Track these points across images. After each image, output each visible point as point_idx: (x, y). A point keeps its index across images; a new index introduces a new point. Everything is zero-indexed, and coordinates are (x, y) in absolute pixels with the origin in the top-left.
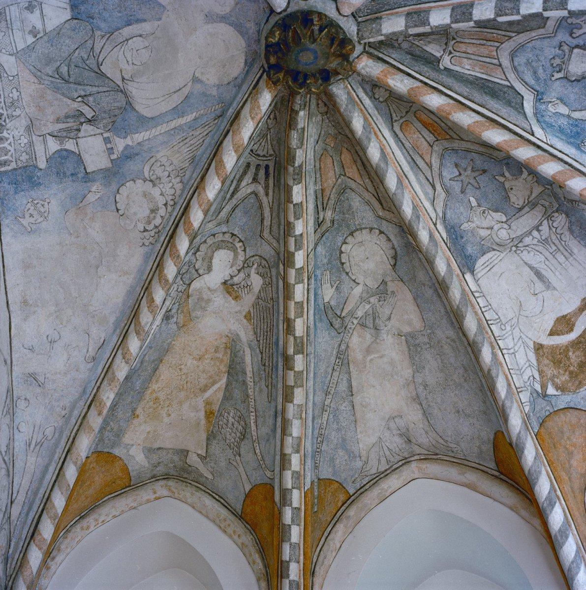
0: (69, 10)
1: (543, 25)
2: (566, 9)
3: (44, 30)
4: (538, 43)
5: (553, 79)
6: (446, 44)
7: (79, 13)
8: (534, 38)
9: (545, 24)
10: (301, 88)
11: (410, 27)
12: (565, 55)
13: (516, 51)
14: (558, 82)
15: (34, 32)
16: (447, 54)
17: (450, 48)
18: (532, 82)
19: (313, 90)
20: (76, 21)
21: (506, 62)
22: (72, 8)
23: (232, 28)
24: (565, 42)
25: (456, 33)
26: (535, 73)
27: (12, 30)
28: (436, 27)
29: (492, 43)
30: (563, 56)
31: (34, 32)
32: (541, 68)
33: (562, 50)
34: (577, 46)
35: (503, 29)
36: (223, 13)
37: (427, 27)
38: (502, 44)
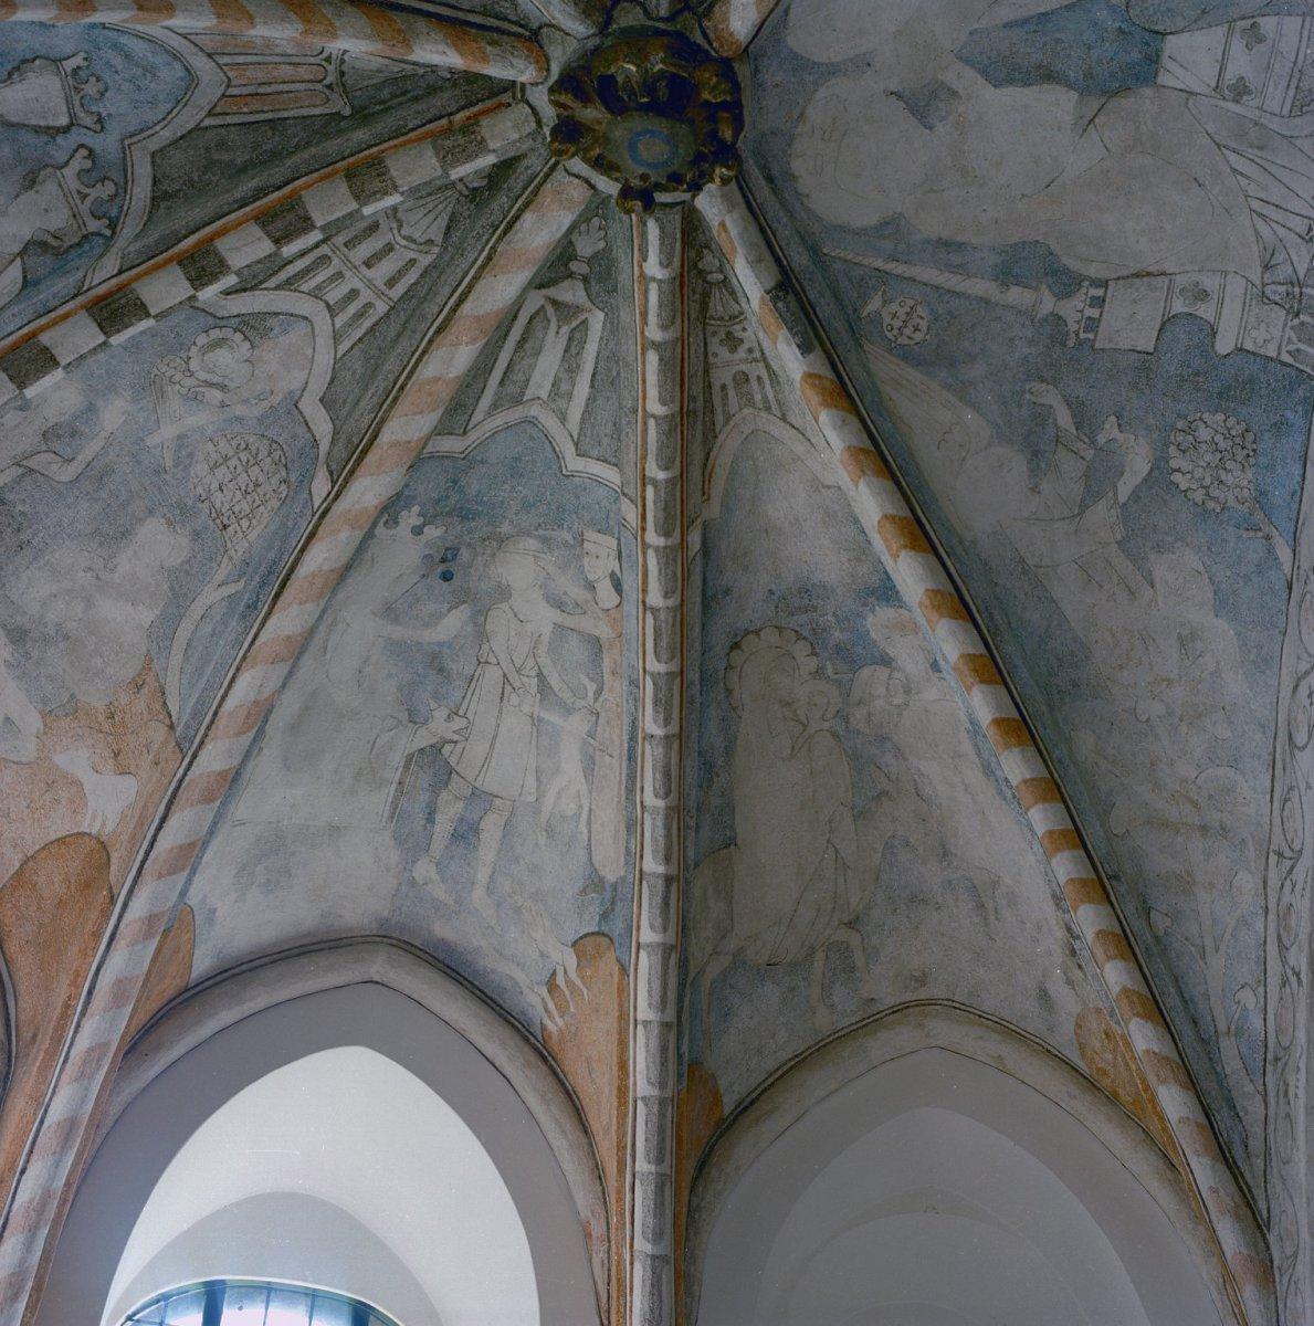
0: (1166, 54)
1: (158, 161)
2: (157, 316)
3: (1230, 32)
4: (150, 116)
5: (82, 55)
6: (342, 74)
7: (1148, 44)
8: (162, 124)
9: (153, 163)
10: (661, 70)
11: (438, 178)
12: (82, 105)
13: (187, 89)
14: (68, 50)
15: (1254, 36)
16: (334, 56)
17: (331, 68)
18: (124, 40)
19: (633, 68)
20: (1159, 28)
21: (201, 63)
22: (1158, 56)
23: (816, 60)
24: (95, 132)
25: (328, 100)
26: (127, 56)
27: (1295, 63)
28: (386, 194)
29: (245, 91)
30: (85, 102)
31: (1254, 36)
32: (120, 68)
33: (92, 113)
34: (66, 130)
35: (233, 129)
36: (834, 81)
37: (405, 188)
38: (223, 95)
